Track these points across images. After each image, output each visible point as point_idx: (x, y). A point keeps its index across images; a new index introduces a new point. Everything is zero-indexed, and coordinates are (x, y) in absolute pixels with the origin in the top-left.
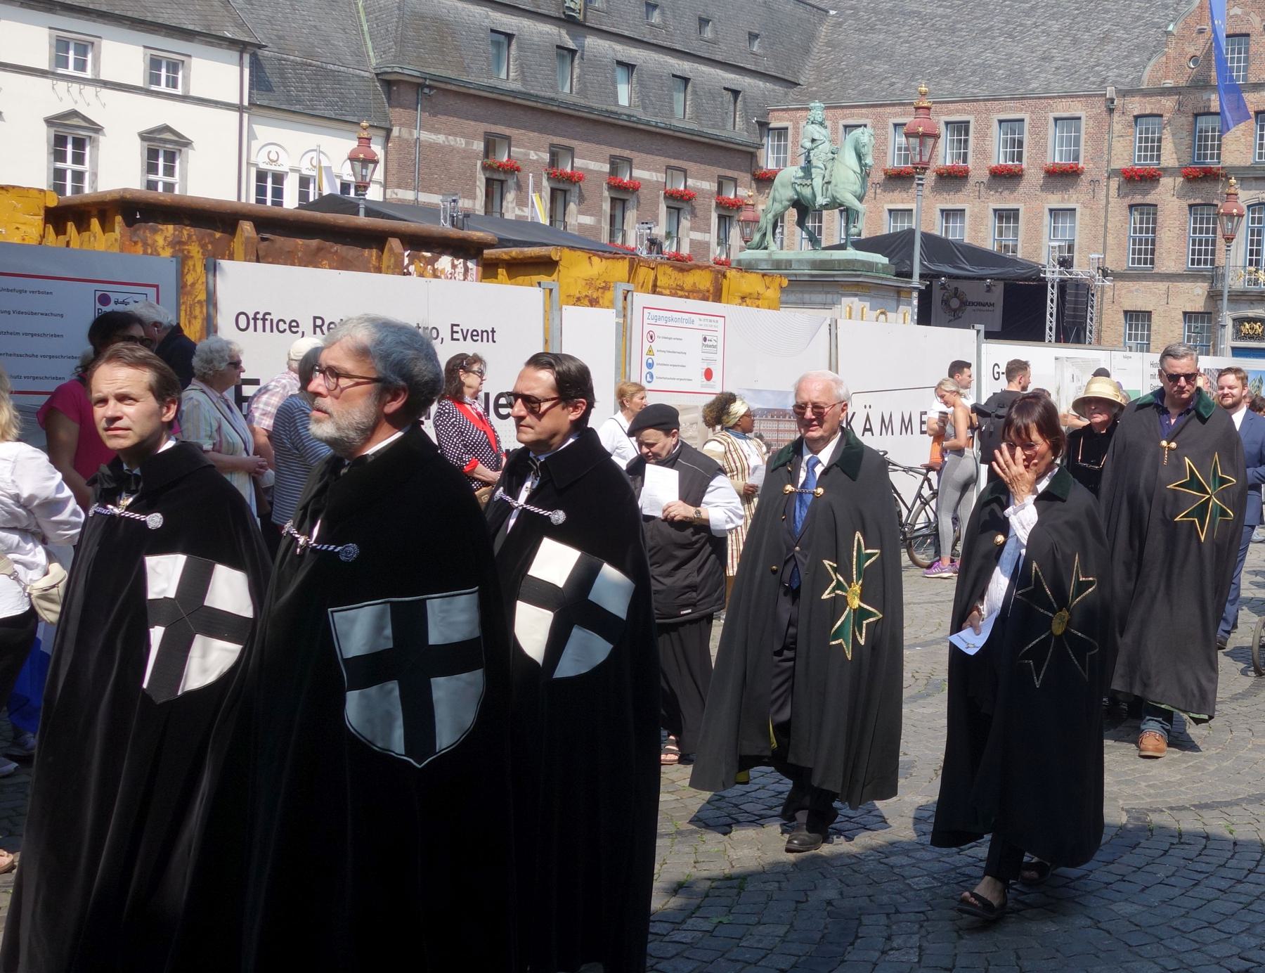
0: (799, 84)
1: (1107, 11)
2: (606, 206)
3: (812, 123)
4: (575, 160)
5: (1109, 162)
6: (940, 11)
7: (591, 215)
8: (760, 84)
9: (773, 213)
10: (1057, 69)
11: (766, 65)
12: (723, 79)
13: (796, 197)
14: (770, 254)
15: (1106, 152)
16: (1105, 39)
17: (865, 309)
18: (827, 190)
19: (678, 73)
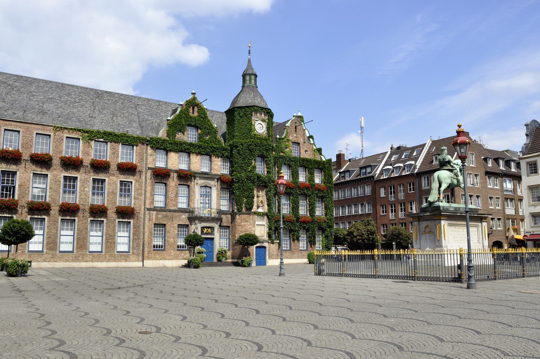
5: (146, 164)
15: (145, 161)
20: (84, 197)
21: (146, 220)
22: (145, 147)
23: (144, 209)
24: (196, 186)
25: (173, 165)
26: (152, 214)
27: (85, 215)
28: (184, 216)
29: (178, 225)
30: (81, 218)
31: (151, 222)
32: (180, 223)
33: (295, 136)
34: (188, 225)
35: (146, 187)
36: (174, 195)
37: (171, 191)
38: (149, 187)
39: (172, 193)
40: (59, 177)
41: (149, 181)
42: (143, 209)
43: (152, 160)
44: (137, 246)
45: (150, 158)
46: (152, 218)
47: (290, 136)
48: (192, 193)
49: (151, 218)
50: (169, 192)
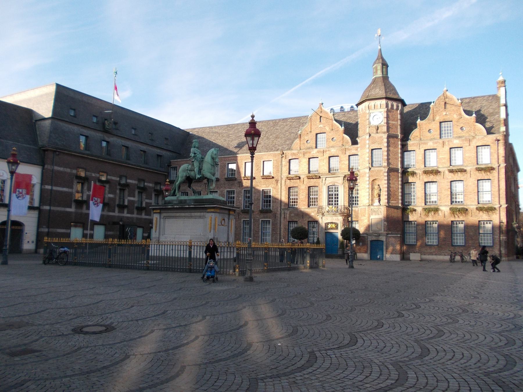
0: (180, 154)
1: (277, 129)
2: (118, 191)
3: (194, 147)
4: (108, 176)
6: (224, 131)
7: (113, 194)
8: (169, 153)
9: (179, 182)
11: (170, 148)
13: (188, 175)
14: (178, 198)
16: (277, 137)
18: (200, 172)
19: (143, 150)
20: (239, 204)
21: (282, 218)
23: (280, 210)
26: (287, 214)
27: (239, 217)
29: (308, 221)
30: (237, 219)
31: (285, 220)
33: (444, 113)
35: (281, 192)
38: (284, 192)
39: (302, 195)
40: (224, 192)
41: (283, 187)
42: (279, 210)
43: (285, 170)
44: (275, 239)
45: (284, 168)
46: (286, 217)
47: (437, 115)
49: (285, 217)
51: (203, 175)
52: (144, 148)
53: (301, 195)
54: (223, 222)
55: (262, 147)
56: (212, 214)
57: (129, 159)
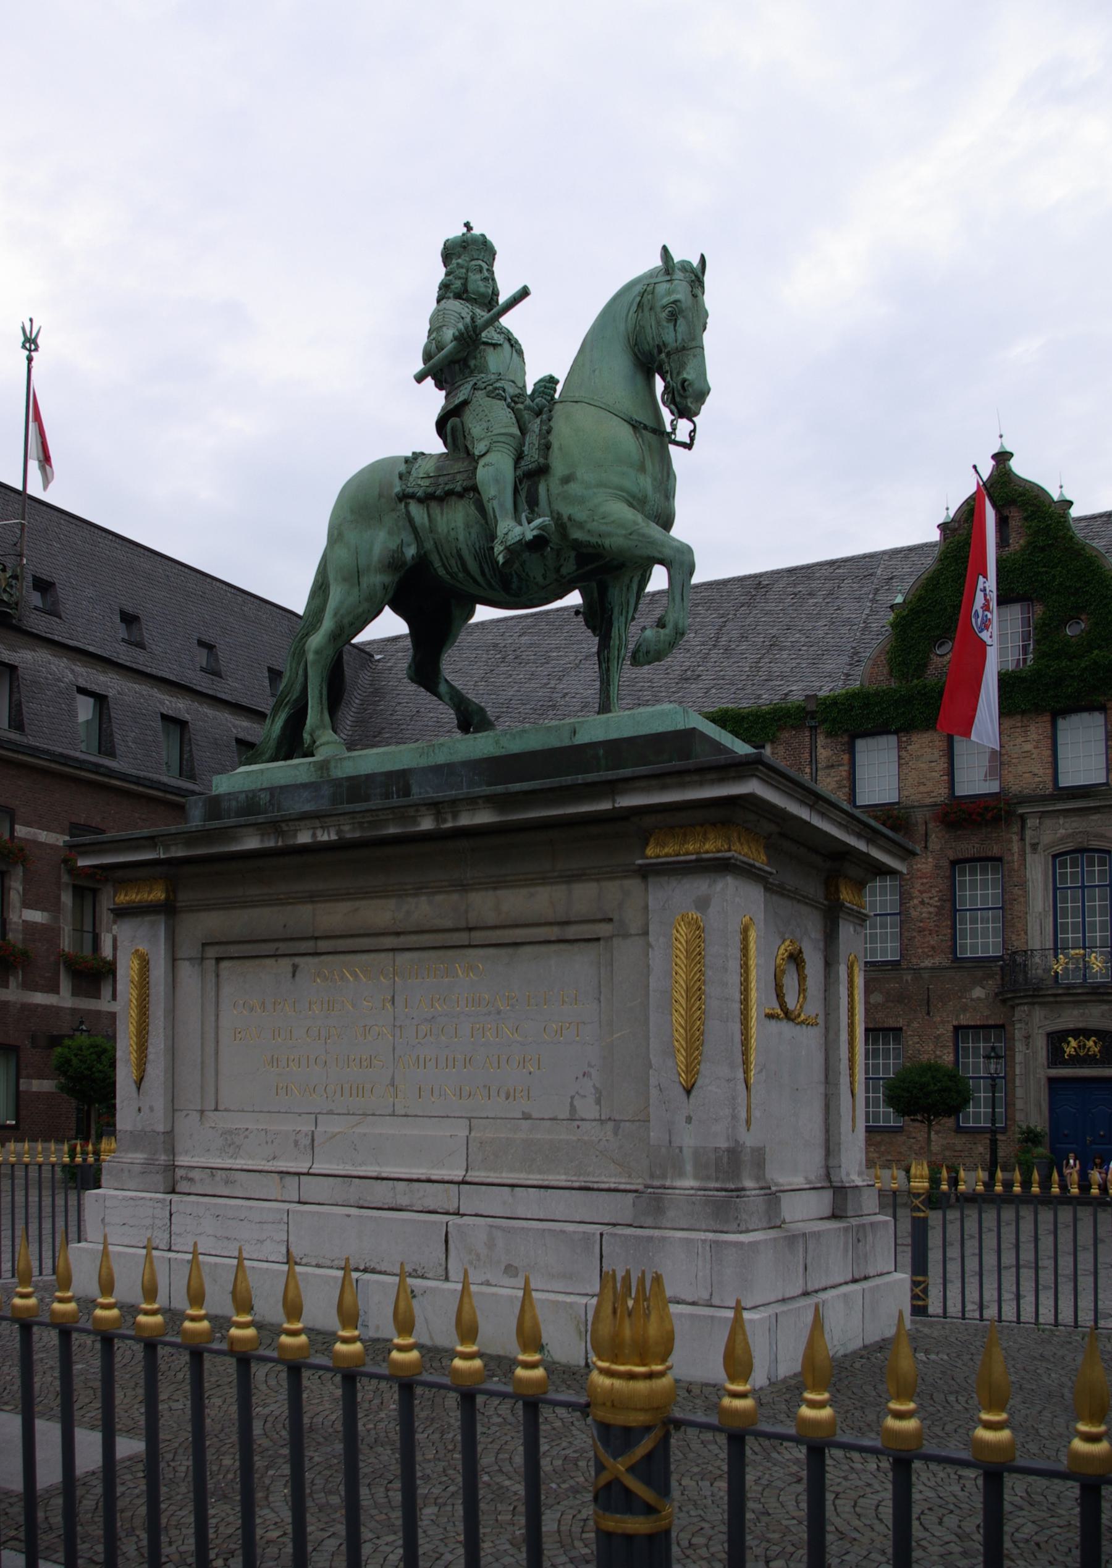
10: (709, 689)
12: (235, 727)
13: (411, 552)
17: (753, 935)
18: (533, 503)
19: (171, 713)
22: (807, 739)
24: (1029, 857)
25: (922, 789)
28: (978, 992)
29: (957, 1029)
32: (964, 1020)
34: (1002, 1026)
36: (932, 909)
37: (917, 893)
39: (922, 903)
43: (834, 785)
45: (828, 780)
48: (1016, 890)
50: (912, 898)
51: (561, 525)
52: (178, 706)
53: (916, 901)
54: (790, 982)
55: (709, 689)
56: (699, 886)
57: (111, 754)
